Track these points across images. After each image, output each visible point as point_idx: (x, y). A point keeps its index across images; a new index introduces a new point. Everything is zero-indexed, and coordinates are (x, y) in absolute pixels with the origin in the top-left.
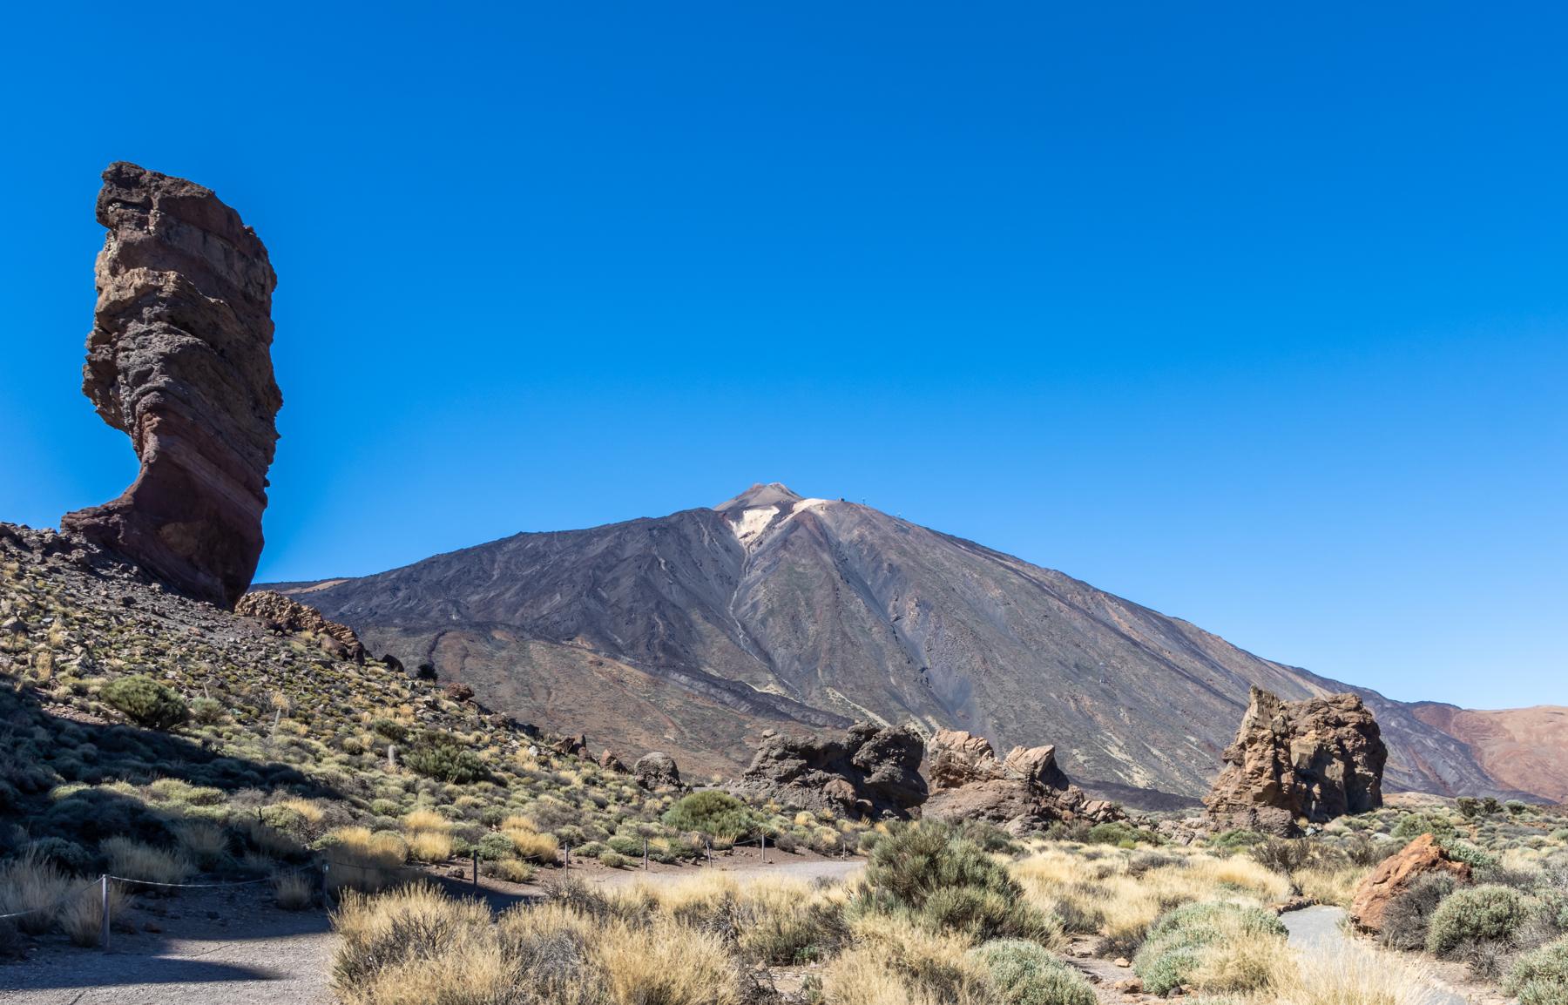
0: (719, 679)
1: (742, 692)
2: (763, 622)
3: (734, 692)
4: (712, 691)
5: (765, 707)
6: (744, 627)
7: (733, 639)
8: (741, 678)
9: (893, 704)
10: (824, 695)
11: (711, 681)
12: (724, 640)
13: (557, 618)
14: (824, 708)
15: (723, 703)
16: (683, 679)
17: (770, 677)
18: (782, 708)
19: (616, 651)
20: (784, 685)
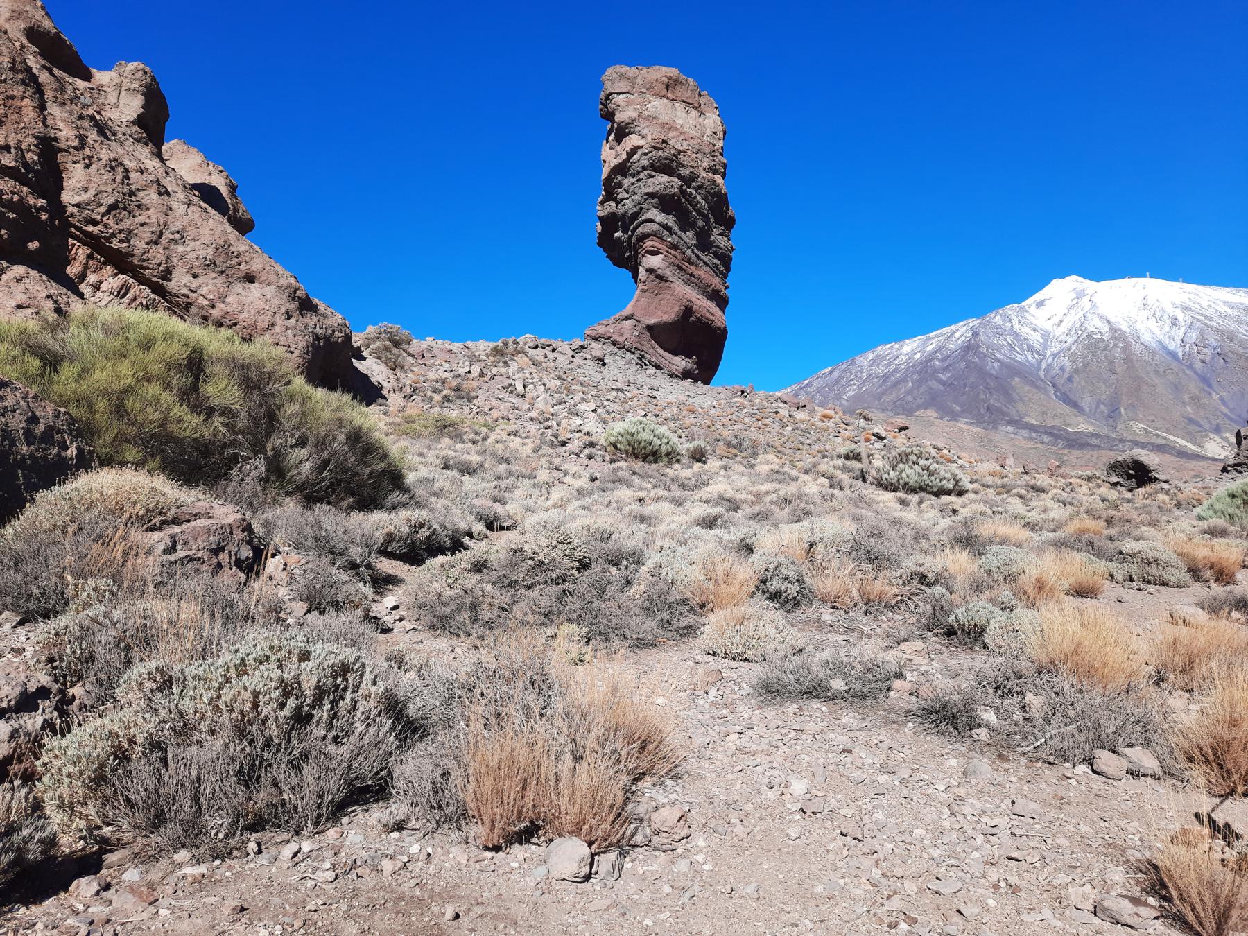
0: (1038, 426)
1: (1055, 434)
2: (1070, 379)
3: (1051, 434)
4: (1034, 435)
5: (1076, 442)
6: (1054, 386)
7: (1046, 393)
8: (1056, 422)
9: (1191, 428)
10: (1127, 427)
11: (1032, 428)
12: (1040, 395)
13: (910, 398)
14: (1130, 438)
15: (1043, 443)
16: (1010, 429)
17: (1080, 419)
18: (1094, 441)
19: (954, 417)
20: (1092, 424)
